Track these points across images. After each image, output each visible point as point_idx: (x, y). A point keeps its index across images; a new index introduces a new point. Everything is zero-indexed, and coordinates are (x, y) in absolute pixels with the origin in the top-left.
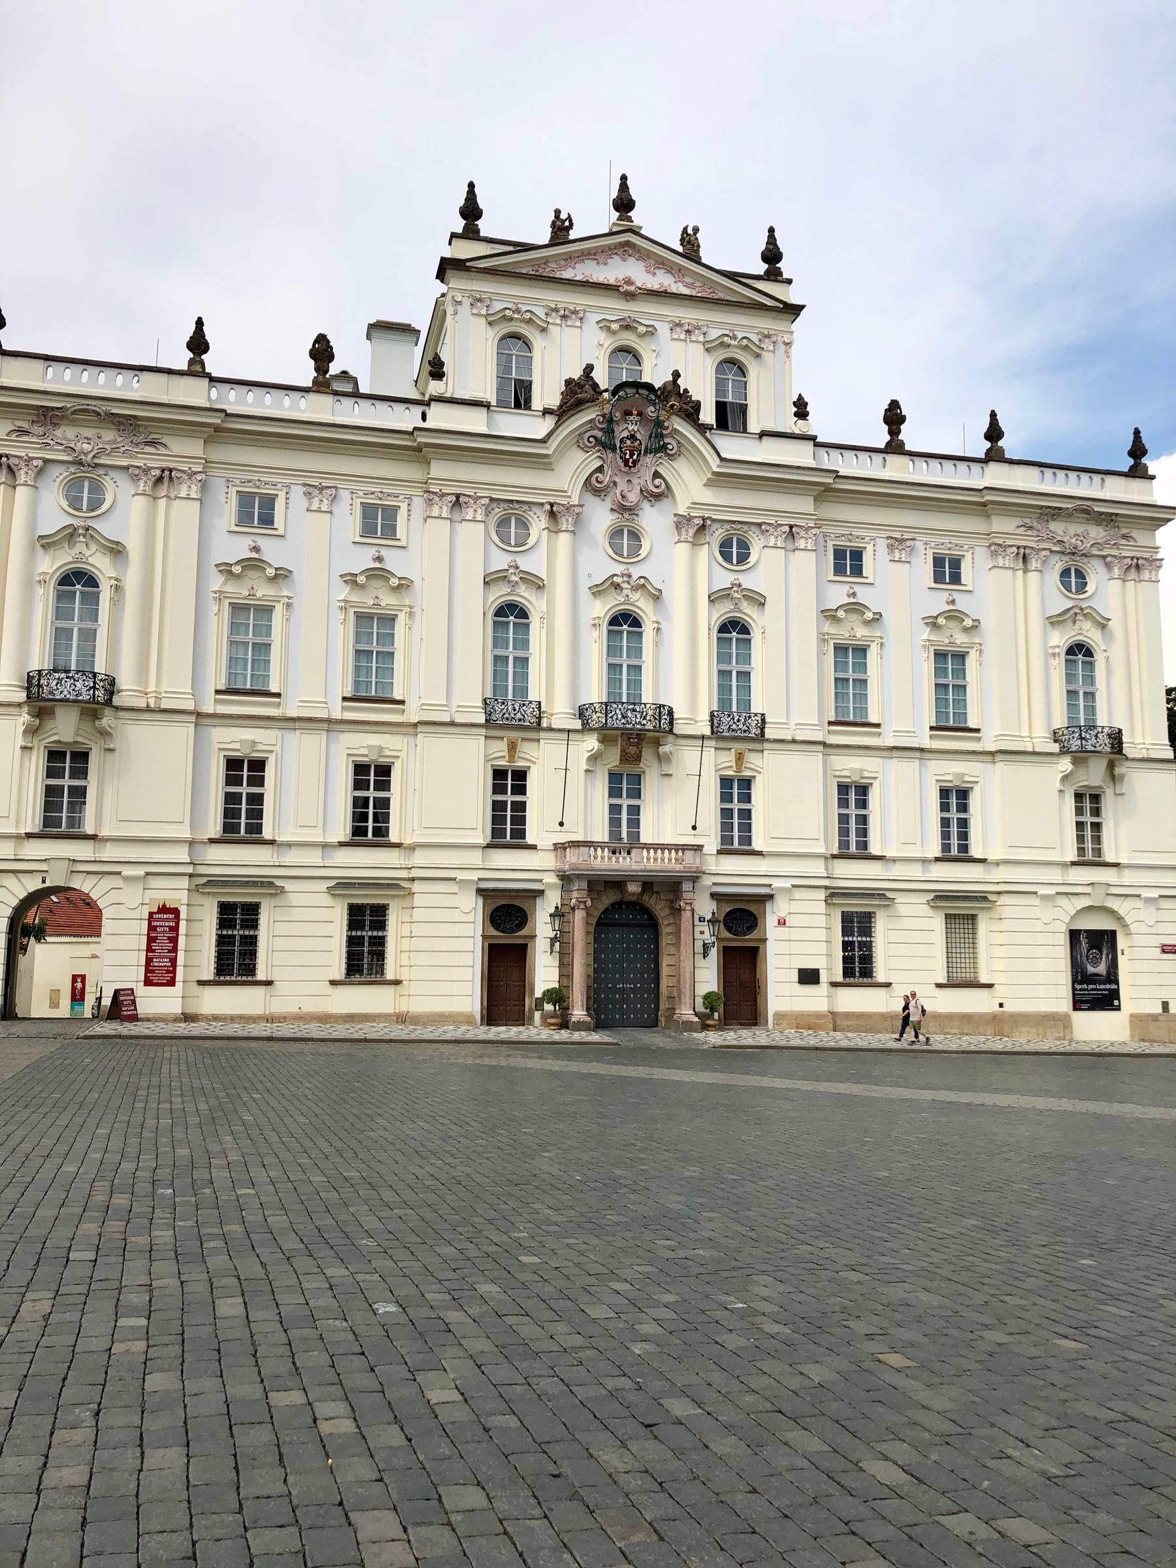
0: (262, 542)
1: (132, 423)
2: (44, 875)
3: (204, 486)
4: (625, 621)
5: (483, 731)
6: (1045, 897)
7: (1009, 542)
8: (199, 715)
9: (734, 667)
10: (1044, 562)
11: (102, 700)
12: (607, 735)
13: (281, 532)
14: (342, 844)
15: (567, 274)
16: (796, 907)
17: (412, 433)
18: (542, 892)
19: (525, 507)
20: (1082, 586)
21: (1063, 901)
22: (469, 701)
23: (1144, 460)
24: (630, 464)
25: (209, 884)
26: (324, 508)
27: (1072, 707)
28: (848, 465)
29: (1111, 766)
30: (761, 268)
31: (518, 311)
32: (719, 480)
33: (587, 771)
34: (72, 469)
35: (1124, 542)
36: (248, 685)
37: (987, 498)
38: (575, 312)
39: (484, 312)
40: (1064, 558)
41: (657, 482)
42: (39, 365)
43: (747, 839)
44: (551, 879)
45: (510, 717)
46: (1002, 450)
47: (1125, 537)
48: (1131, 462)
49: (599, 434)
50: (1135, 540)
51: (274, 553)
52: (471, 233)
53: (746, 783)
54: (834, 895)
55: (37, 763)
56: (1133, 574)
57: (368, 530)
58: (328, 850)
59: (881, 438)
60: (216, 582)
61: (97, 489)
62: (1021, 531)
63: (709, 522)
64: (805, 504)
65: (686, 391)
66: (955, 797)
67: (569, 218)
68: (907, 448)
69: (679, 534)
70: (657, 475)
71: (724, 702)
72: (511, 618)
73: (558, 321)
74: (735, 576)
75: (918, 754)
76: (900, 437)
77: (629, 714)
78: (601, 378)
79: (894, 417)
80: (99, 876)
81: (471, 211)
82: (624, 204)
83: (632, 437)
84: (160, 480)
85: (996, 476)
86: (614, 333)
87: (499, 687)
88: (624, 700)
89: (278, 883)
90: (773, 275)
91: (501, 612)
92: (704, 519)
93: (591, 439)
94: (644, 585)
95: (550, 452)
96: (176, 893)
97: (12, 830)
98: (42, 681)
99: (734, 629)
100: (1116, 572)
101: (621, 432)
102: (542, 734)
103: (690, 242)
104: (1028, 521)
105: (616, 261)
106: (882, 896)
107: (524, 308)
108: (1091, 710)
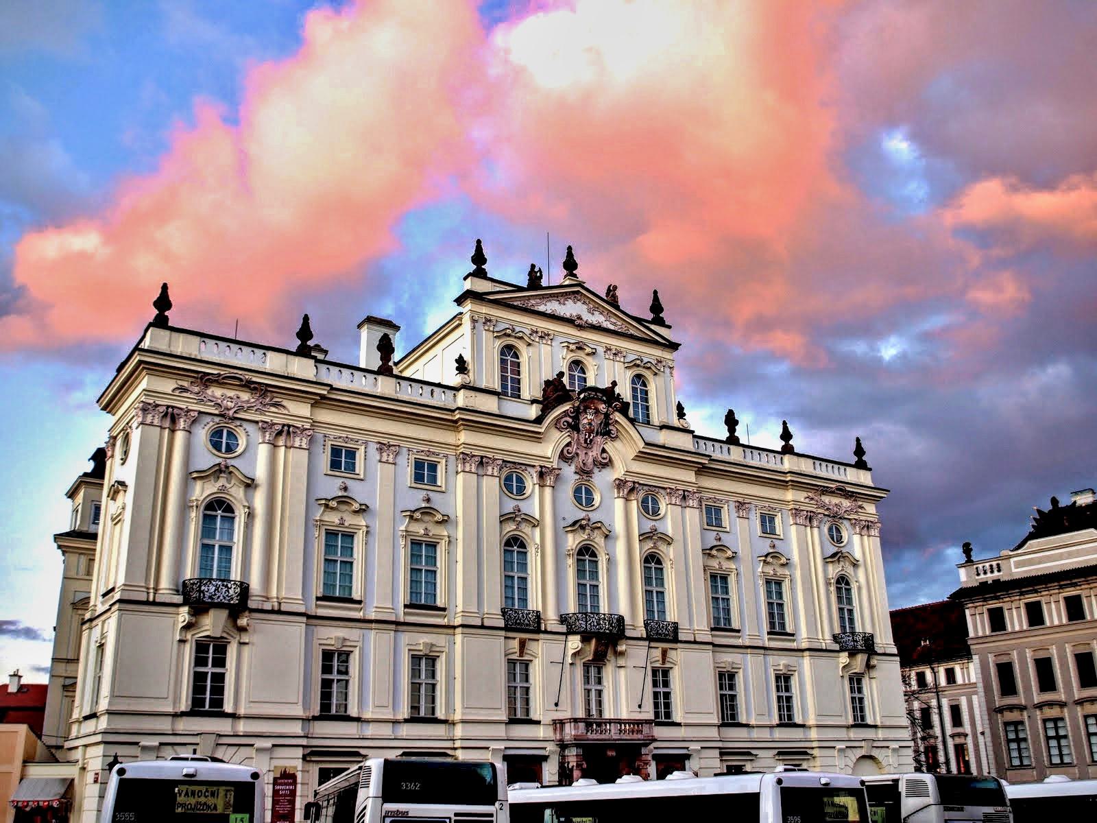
0: (349, 483)
1: (265, 390)
2: (195, 747)
3: (312, 440)
4: (586, 552)
5: (503, 633)
6: (840, 750)
7: (802, 508)
8: (309, 617)
9: (847, 607)
10: (820, 522)
11: (240, 606)
12: (586, 639)
13: (362, 477)
14: (406, 721)
15: (542, 308)
16: (704, 763)
17: (453, 411)
18: (545, 758)
19: (523, 467)
20: (840, 540)
21: (849, 752)
22: (492, 608)
23: (864, 458)
24: (589, 444)
25: (313, 753)
26: (391, 460)
28: (709, 449)
29: (868, 660)
30: (650, 316)
31: (513, 330)
32: (641, 457)
33: (571, 664)
34: (217, 419)
35: (860, 510)
36: (337, 592)
38: (549, 335)
39: (491, 329)
40: (830, 519)
41: (604, 455)
42: (197, 339)
43: (668, 715)
44: (551, 748)
45: (521, 624)
46: (792, 448)
47: (861, 507)
48: (856, 459)
49: (570, 420)
50: (865, 509)
51: (358, 492)
52: (480, 273)
53: (666, 673)
54: (723, 753)
55: (188, 652)
56: (865, 532)
57: (418, 478)
58: (398, 726)
59: (723, 434)
60: (318, 513)
61: (231, 435)
62: (807, 500)
63: (637, 485)
64: (689, 476)
65: (619, 395)
66: (783, 681)
67: (540, 270)
68: (741, 442)
69: (619, 493)
70: (604, 451)
71: (649, 611)
72: (515, 548)
73: (537, 340)
74: (654, 523)
75: (762, 651)
76: (736, 434)
77: (601, 622)
78: (565, 380)
79: (731, 421)
80: (237, 747)
81: (479, 258)
82: (570, 265)
83: (590, 424)
84: (280, 433)
85: (788, 463)
86: (572, 351)
87: (509, 598)
88: (589, 611)
89: (363, 752)
90: (660, 321)
91: (508, 543)
92: (634, 482)
93: (565, 423)
94: (600, 528)
95: (542, 430)
96: (292, 760)
97: (170, 709)
98: (203, 588)
99: (653, 561)
100: (858, 530)
101: (584, 421)
102: (542, 636)
103: (612, 298)
104: (810, 494)
105: (570, 303)
106: (750, 754)
107: (518, 329)
108: (851, 621)
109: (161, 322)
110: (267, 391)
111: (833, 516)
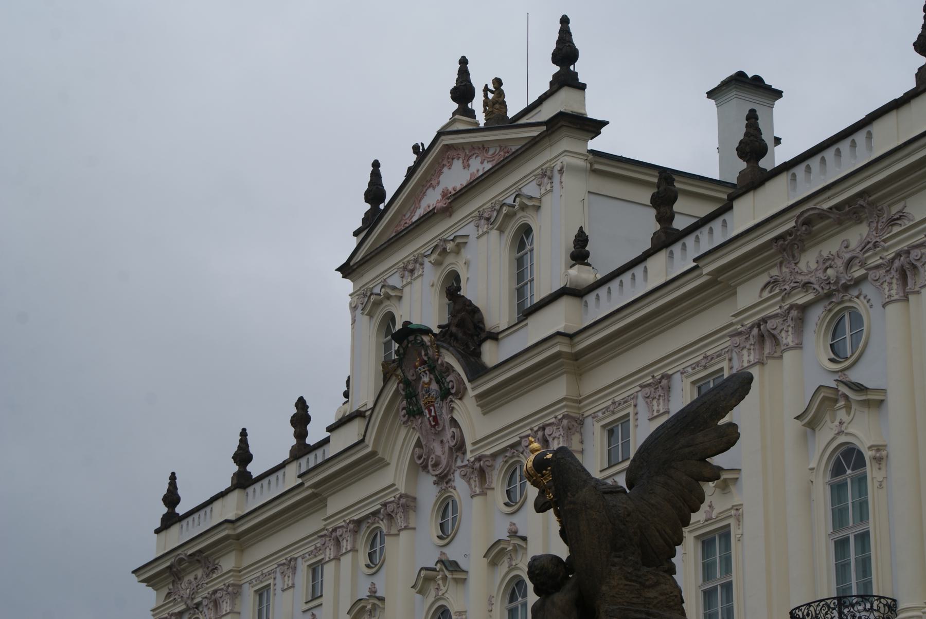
7: (748, 323)
27: (842, 570)
35: (896, 229)
37: (706, 270)
38: (416, 261)
47: (892, 222)
62: (766, 294)
64: (557, 390)
82: (462, 92)
95: (369, 450)
104: (775, 272)
109: (170, 520)
110: (207, 558)
111: (829, 295)
